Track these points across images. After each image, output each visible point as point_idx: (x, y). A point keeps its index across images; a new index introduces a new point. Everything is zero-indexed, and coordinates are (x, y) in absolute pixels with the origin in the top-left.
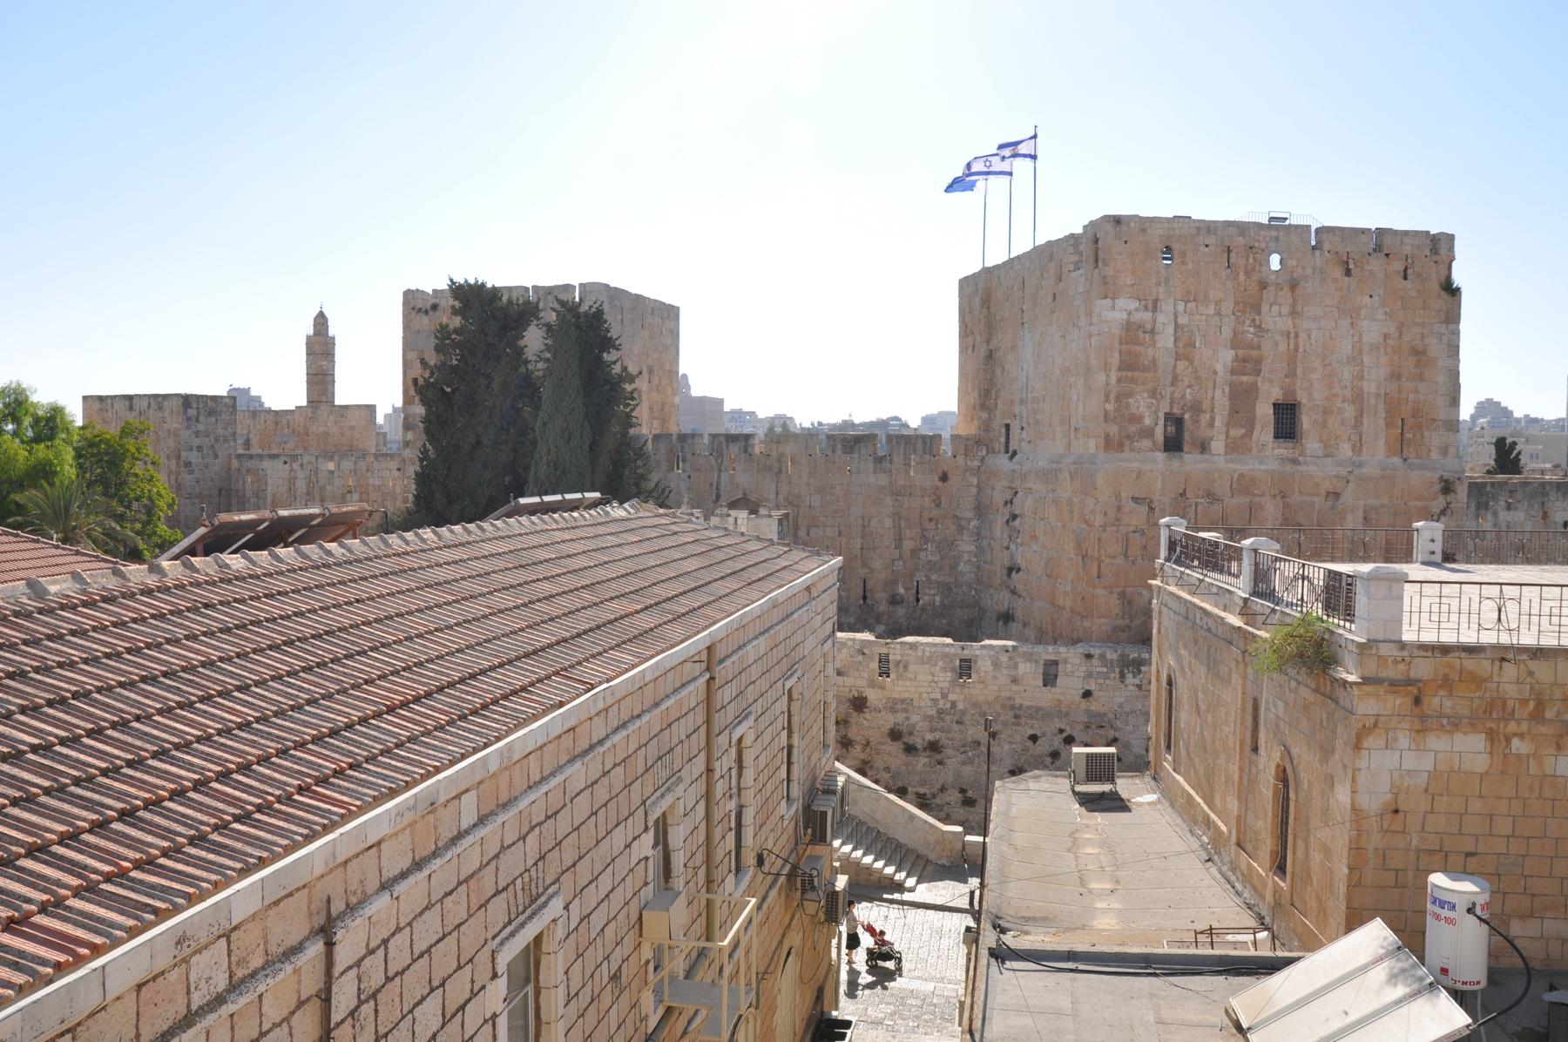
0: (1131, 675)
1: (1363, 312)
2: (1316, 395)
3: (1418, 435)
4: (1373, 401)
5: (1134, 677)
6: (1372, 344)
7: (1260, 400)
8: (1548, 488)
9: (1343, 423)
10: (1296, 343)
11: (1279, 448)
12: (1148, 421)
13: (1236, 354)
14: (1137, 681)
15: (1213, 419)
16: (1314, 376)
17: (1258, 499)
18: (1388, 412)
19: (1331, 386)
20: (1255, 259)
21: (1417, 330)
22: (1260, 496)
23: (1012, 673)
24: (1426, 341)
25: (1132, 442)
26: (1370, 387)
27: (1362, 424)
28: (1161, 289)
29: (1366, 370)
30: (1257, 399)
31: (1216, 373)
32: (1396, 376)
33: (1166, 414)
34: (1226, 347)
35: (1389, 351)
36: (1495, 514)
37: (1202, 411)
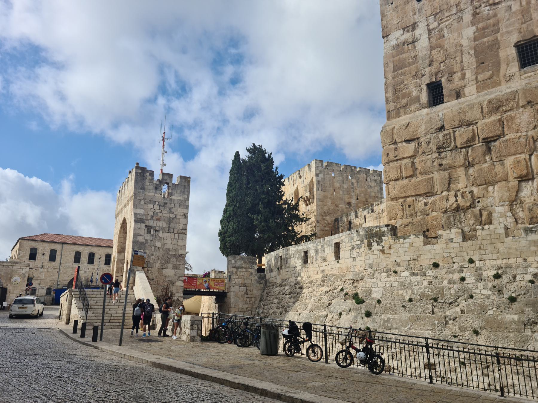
0: (375, 244)
5: (378, 244)
7: (502, 47)
13: (477, 28)
14: (380, 247)
22: (510, 110)
23: (323, 255)
25: (406, 109)
28: (416, 16)
30: (499, 48)
31: (461, 46)
33: (428, 85)
34: (469, 26)
37: (455, 73)
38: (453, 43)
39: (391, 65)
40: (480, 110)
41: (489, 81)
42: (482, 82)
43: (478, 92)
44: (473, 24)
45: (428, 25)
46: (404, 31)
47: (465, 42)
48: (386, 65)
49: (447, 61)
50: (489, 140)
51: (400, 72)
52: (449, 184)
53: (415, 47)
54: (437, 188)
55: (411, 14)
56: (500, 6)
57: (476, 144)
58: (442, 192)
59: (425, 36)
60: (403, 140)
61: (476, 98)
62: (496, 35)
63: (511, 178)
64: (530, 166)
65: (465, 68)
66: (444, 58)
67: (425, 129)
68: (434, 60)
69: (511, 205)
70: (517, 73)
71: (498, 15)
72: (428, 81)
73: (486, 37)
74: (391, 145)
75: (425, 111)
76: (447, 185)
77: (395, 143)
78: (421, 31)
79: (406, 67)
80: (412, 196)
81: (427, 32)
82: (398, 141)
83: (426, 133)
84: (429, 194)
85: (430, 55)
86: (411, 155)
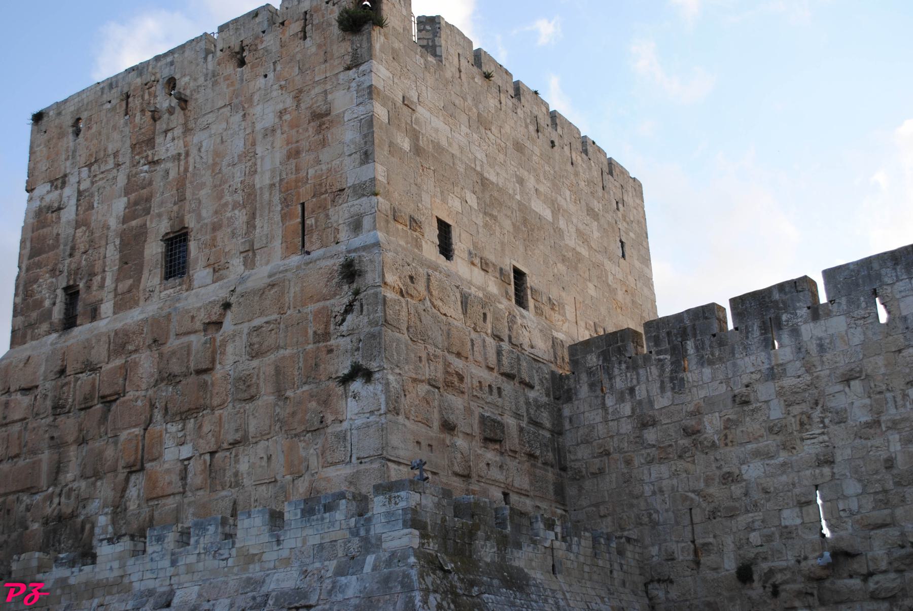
1: (256, 98)
2: (204, 213)
3: (322, 216)
4: (266, 196)
6: (266, 129)
8: (876, 266)
9: (233, 235)
10: (187, 162)
11: (165, 289)
12: (47, 303)
15: (103, 279)
16: (203, 193)
17: (133, 356)
18: (285, 202)
19: (220, 197)
20: (150, 94)
21: (318, 89)
22: (136, 351)
24: (330, 97)
25: (34, 329)
26: (262, 180)
27: (255, 227)
28: (68, 163)
29: (259, 162)
30: (145, 241)
31: (108, 229)
32: (294, 154)
34: (120, 196)
35: (286, 128)
36: (795, 332)
37: (95, 275)
38: (100, 221)
39: (28, 244)
40: (107, 345)
41: (128, 295)
42: (121, 297)
43: (115, 313)
44: (127, 191)
45: (79, 182)
46: (51, 186)
47: (113, 223)
48: (23, 242)
49: (90, 252)
50: (108, 399)
51: (37, 259)
52: (57, 473)
53: (59, 218)
54: (44, 481)
55: (64, 157)
56: (158, 168)
57: (95, 405)
58: (48, 488)
59: (73, 201)
60: (18, 388)
61: (107, 324)
62: (145, 218)
63: (120, 468)
64: (141, 448)
65: (106, 269)
66: (87, 246)
67: (45, 372)
68: (77, 247)
69: (115, 513)
70: (158, 287)
71: (154, 183)
72: (64, 285)
73: (135, 219)
74: (4, 396)
75: (54, 336)
76: (54, 475)
77: (8, 392)
78: (69, 192)
79: (45, 252)
80: (14, 492)
81: (76, 195)
82: (12, 389)
83: (45, 379)
84: (31, 490)
85: (74, 236)
86: (21, 416)
